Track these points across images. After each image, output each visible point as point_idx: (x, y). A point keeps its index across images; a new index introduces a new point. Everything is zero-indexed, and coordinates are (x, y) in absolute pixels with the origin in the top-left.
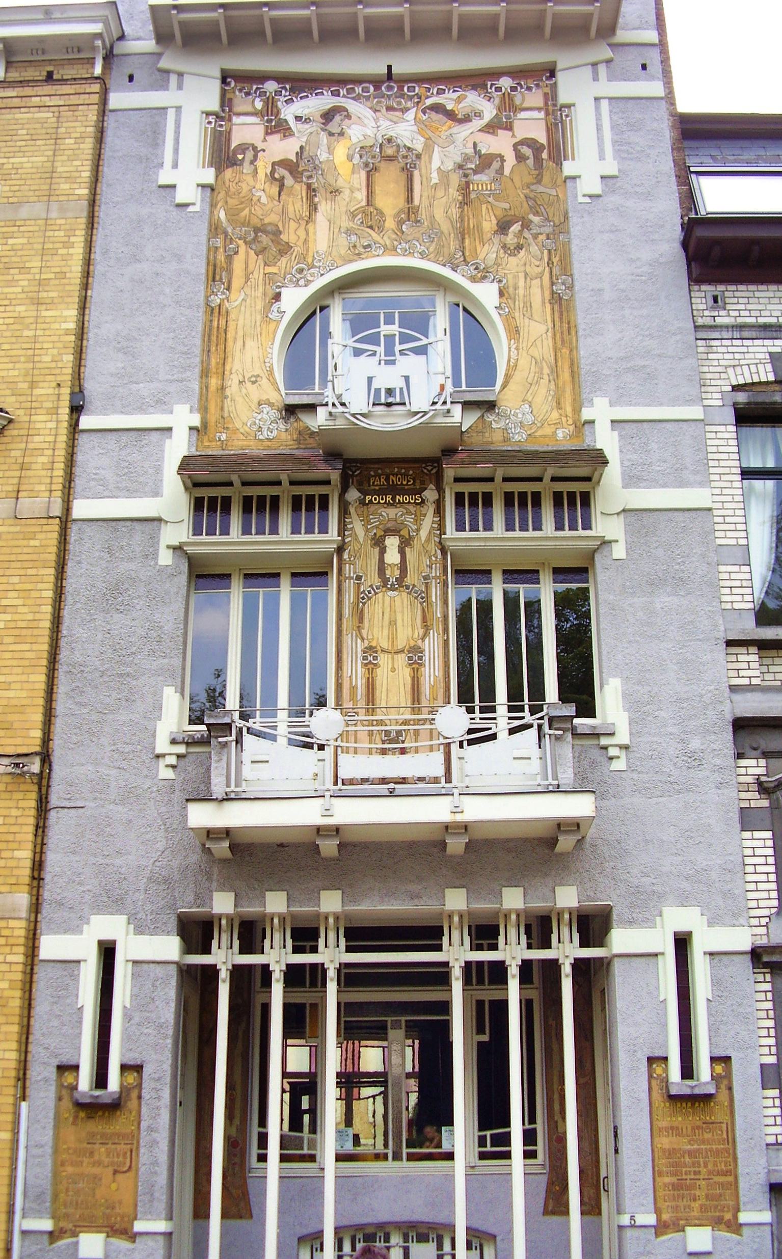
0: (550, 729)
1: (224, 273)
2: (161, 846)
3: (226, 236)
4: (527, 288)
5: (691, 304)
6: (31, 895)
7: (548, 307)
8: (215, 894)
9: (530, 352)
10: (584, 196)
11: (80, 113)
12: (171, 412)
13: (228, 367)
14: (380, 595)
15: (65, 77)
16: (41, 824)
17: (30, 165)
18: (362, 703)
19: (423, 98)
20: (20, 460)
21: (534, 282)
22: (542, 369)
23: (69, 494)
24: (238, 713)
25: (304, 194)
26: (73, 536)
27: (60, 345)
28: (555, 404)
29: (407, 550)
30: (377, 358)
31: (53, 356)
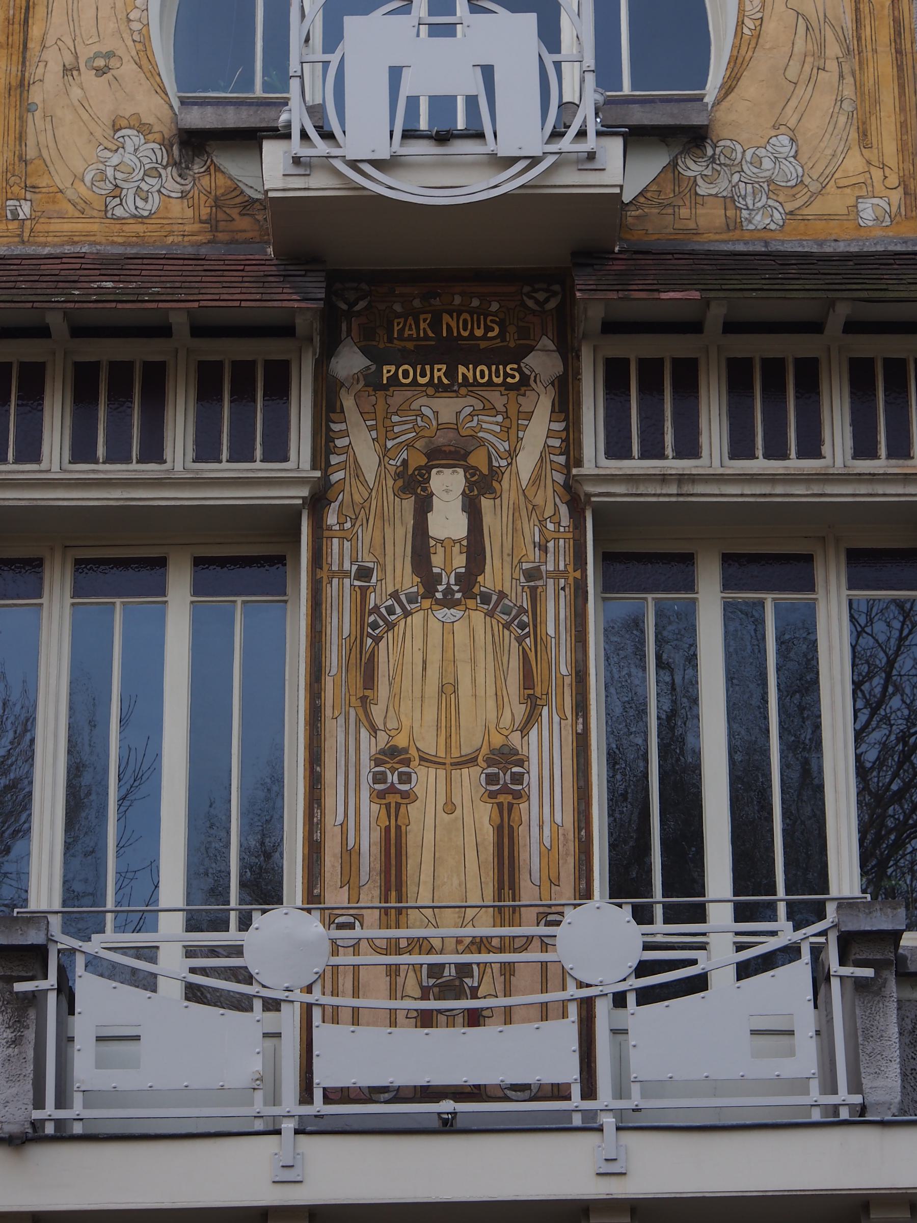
0: (842, 963)
13: (35, 31)
18: (370, 896)
22: (822, 45)
28: (854, 135)
29: (486, 503)
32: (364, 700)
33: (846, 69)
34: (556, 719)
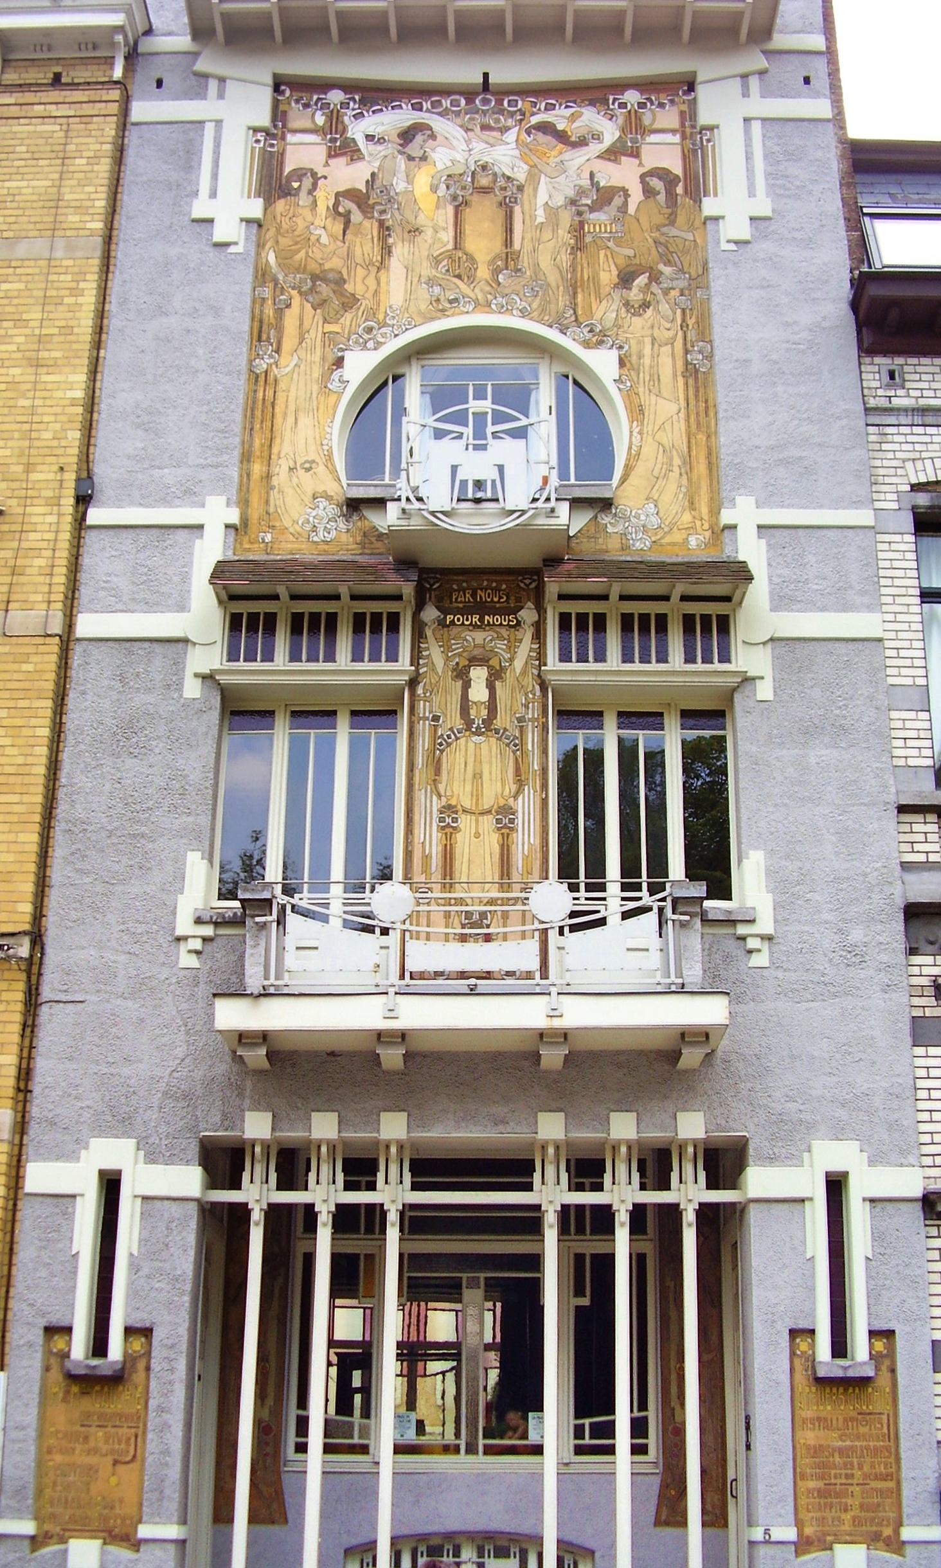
0: (673, 913)
1: (272, 331)
2: (180, 1052)
3: (276, 285)
4: (655, 356)
5: (862, 380)
6: (16, 1111)
7: (681, 380)
8: (247, 1113)
9: (657, 437)
10: (728, 241)
11: (95, 126)
12: (203, 506)
13: (275, 450)
14: (463, 741)
15: (76, 81)
16: (30, 1022)
17: (30, 191)
18: (437, 877)
19: (527, 114)
20: (11, 563)
21: (664, 349)
22: (671, 459)
23: (72, 607)
24: (280, 886)
25: (375, 234)
26: (76, 660)
27: (64, 418)
28: (687, 503)
29: (498, 684)
30: (463, 442)
31: (55, 431)
32: (435, 780)
33: (683, 470)
34: (532, 791)
